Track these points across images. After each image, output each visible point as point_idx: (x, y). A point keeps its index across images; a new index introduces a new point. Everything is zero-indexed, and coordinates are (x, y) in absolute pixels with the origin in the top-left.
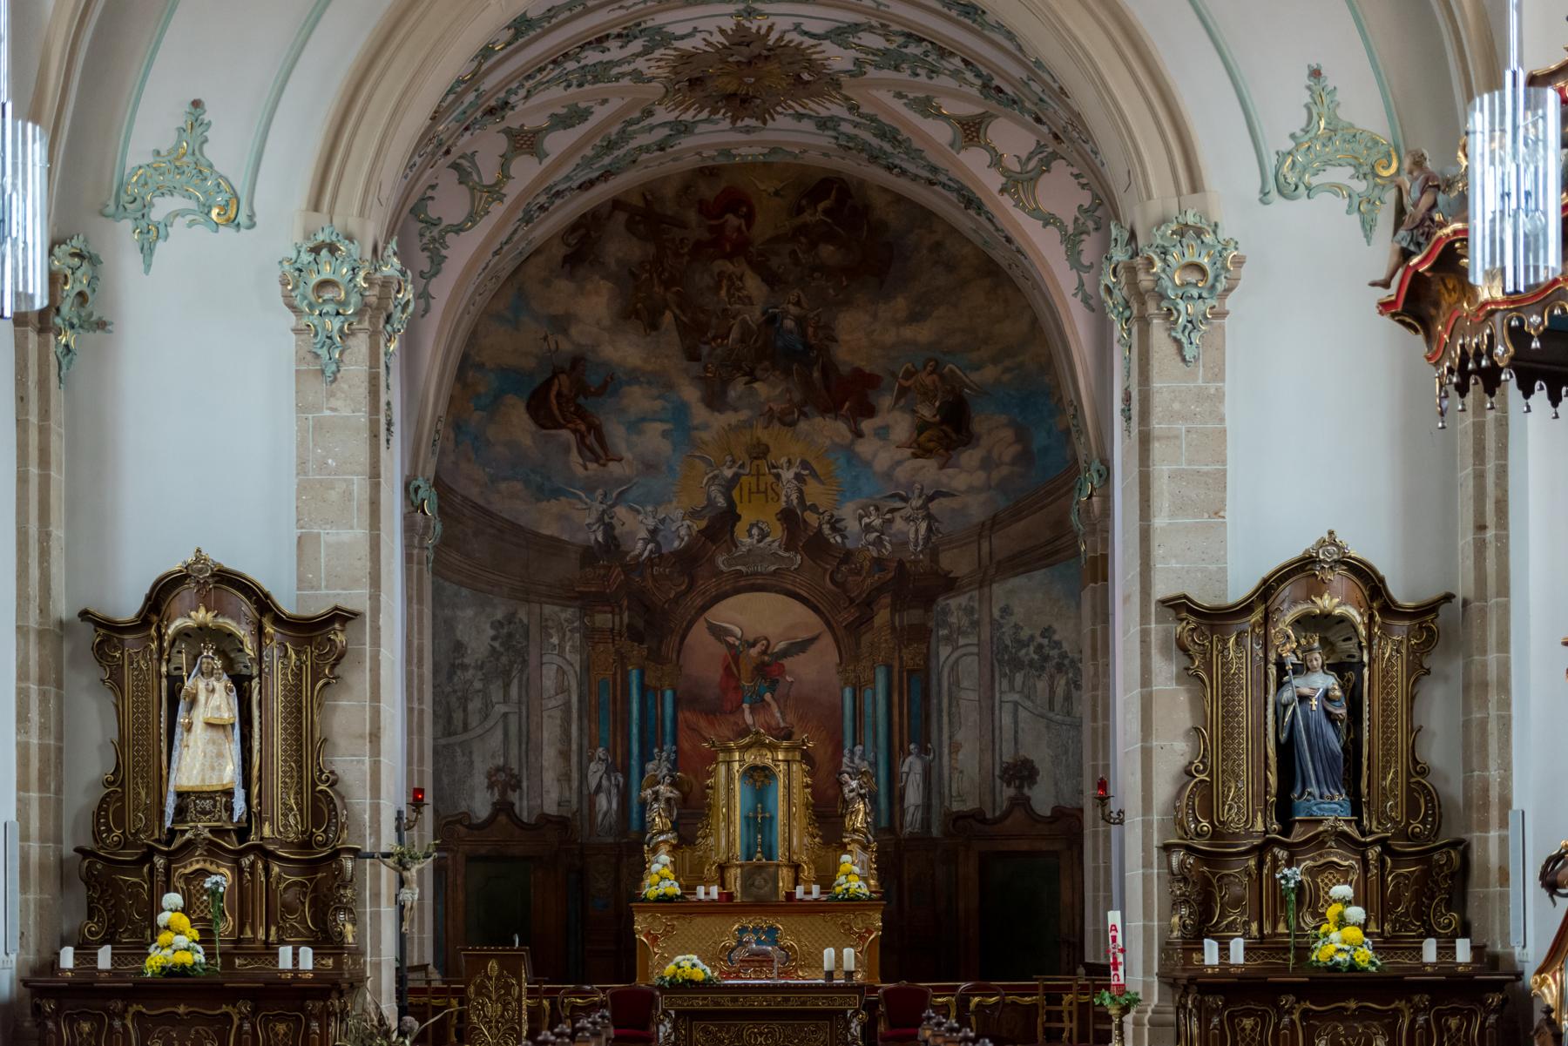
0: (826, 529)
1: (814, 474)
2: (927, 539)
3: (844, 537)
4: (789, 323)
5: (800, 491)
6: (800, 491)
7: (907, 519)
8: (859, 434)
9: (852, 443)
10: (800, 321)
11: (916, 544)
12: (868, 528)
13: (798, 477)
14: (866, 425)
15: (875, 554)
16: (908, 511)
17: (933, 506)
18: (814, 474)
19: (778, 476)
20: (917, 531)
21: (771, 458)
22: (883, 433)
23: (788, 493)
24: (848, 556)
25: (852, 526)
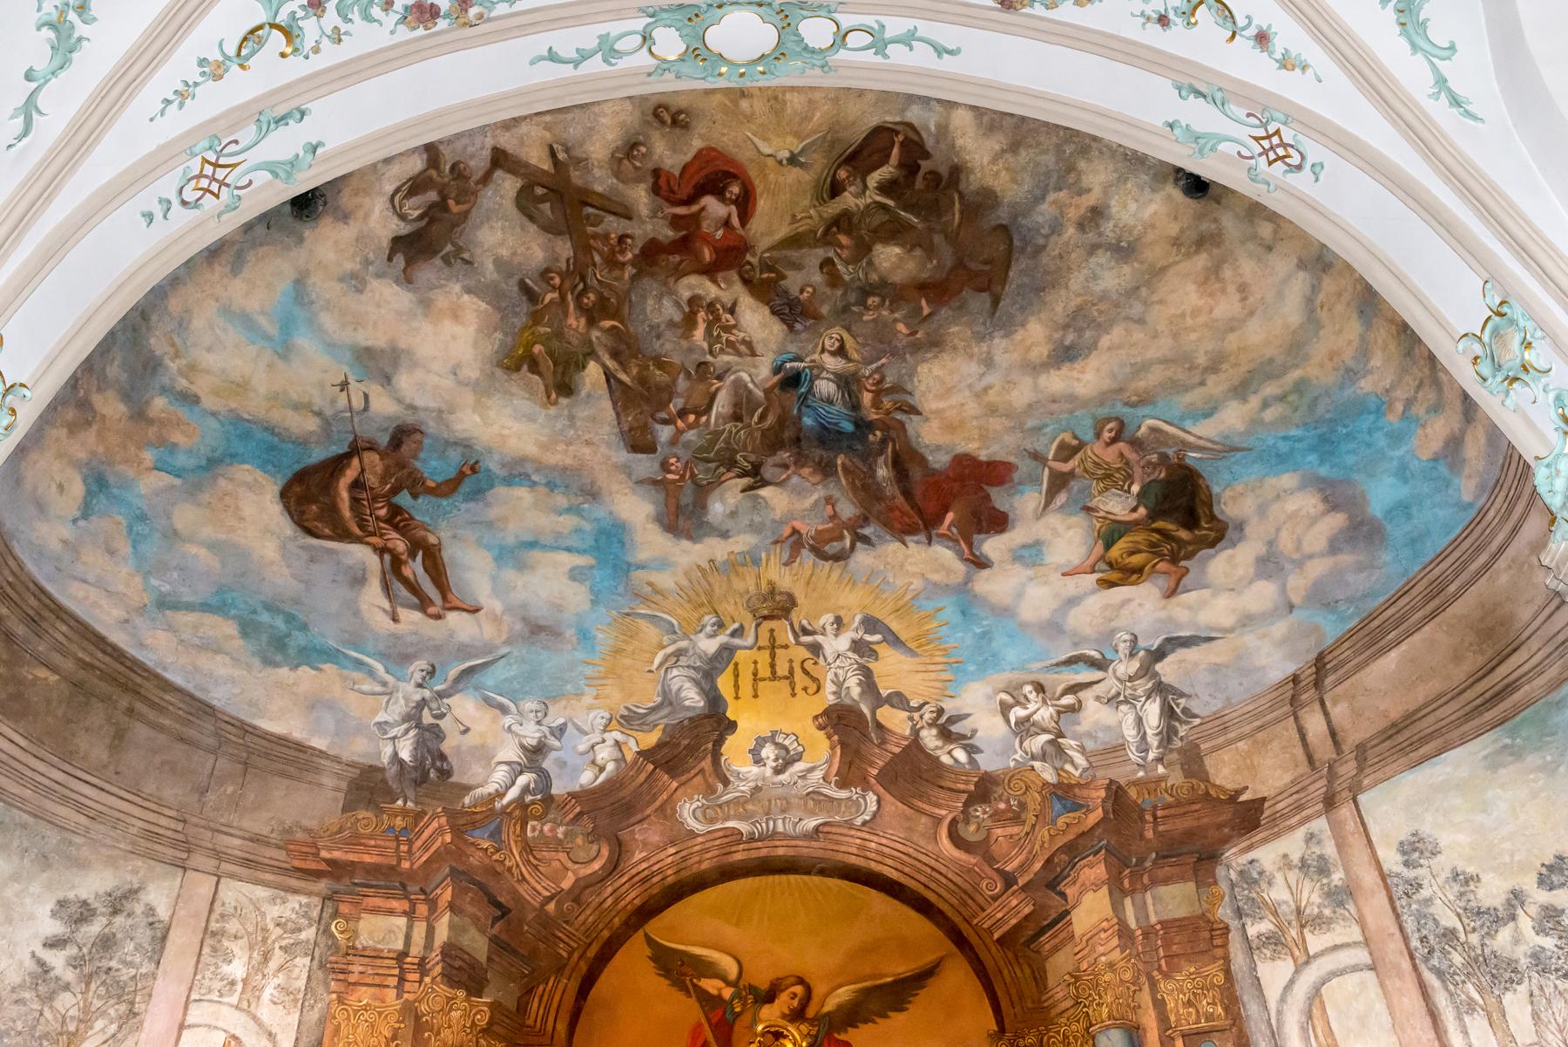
0: (930, 738)
1: (894, 640)
2: (1167, 735)
3: (971, 750)
4: (825, 387)
5: (867, 673)
6: (867, 673)
7: (1114, 701)
8: (980, 563)
9: (968, 579)
10: (847, 383)
11: (1144, 747)
12: (1025, 728)
13: (858, 646)
14: (992, 546)
15: (1049, 776)
16: (1110, 685)
17: (1167, 669)
18: (894, 640)
19: (816, 649)
20: (1139, 721)
21: (799, 617)
22: (1031, 554)
23: (840, 676)
24: (985, 788)
25: (988, 727)
